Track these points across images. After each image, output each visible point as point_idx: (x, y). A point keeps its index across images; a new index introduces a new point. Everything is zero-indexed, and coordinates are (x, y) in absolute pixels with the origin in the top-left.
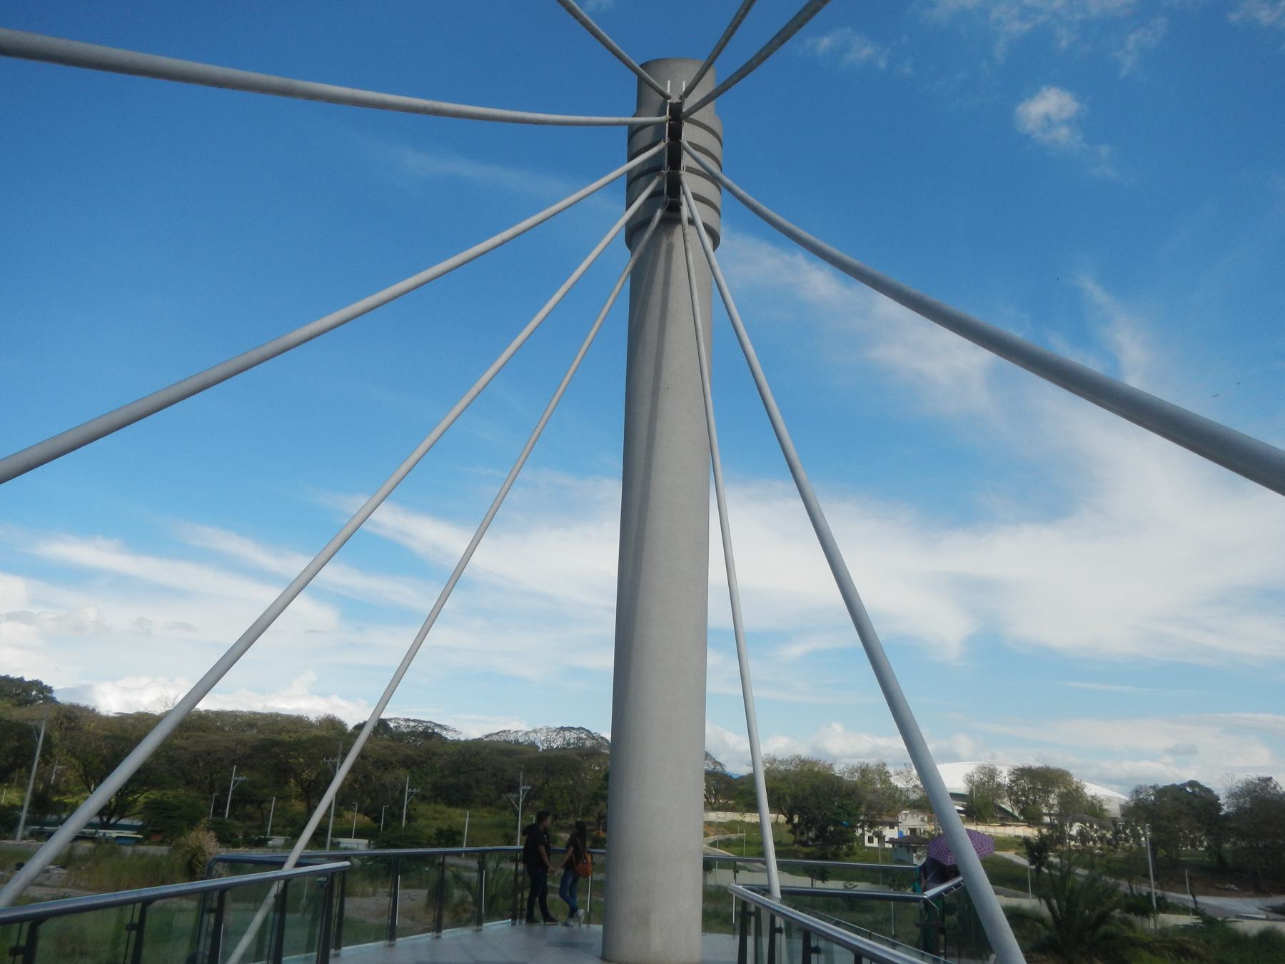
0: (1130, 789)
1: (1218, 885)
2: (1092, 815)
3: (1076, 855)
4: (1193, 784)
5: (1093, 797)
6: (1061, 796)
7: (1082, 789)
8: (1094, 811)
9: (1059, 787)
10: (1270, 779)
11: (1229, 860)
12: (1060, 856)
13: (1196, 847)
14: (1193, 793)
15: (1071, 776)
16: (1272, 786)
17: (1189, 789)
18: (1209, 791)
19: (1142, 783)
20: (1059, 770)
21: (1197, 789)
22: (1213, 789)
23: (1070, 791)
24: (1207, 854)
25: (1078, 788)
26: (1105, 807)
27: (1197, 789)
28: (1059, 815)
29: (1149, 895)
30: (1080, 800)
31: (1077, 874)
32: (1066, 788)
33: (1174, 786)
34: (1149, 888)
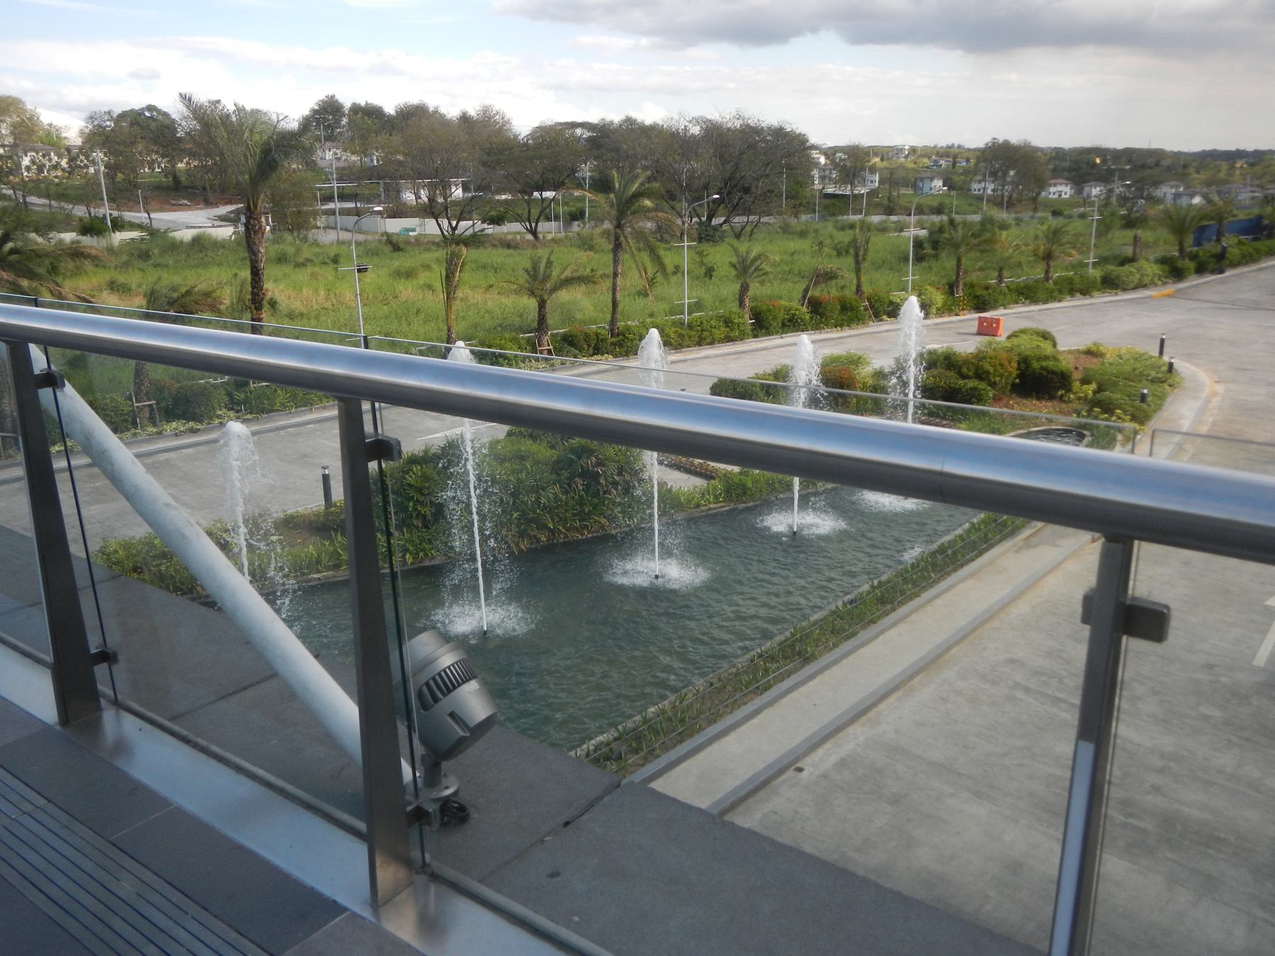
0: (85, 115)
1: (173, 202)
2: (49, 145)
3: (30, 185)
4: (151, 108)
5: (50, 125)
6: (14, 126)
7: (38, 118)
8: (52, 141)
9: (10, 116)
10: (218, 102)
11: (183, 179)
12: (13, 188)
13: (152, 169)
14: (151, 117)
15: (23, 103)
16: (221, 108)
17: (147, 114)
18: (166, 115)
19: (96, 109)
20: (9, 97)
21: (155, 113)
22: (170, 113)
23: (23, 121)
24: (163, 174)
25: (32, 116)
26: (64, 135)
27: (155, 113)
28: (14, 146)
29: (105, 216)
30: (36, 129)
31: (34, 204)
32: (18, 116)
33: (132, 110)
34: (105, 210)
